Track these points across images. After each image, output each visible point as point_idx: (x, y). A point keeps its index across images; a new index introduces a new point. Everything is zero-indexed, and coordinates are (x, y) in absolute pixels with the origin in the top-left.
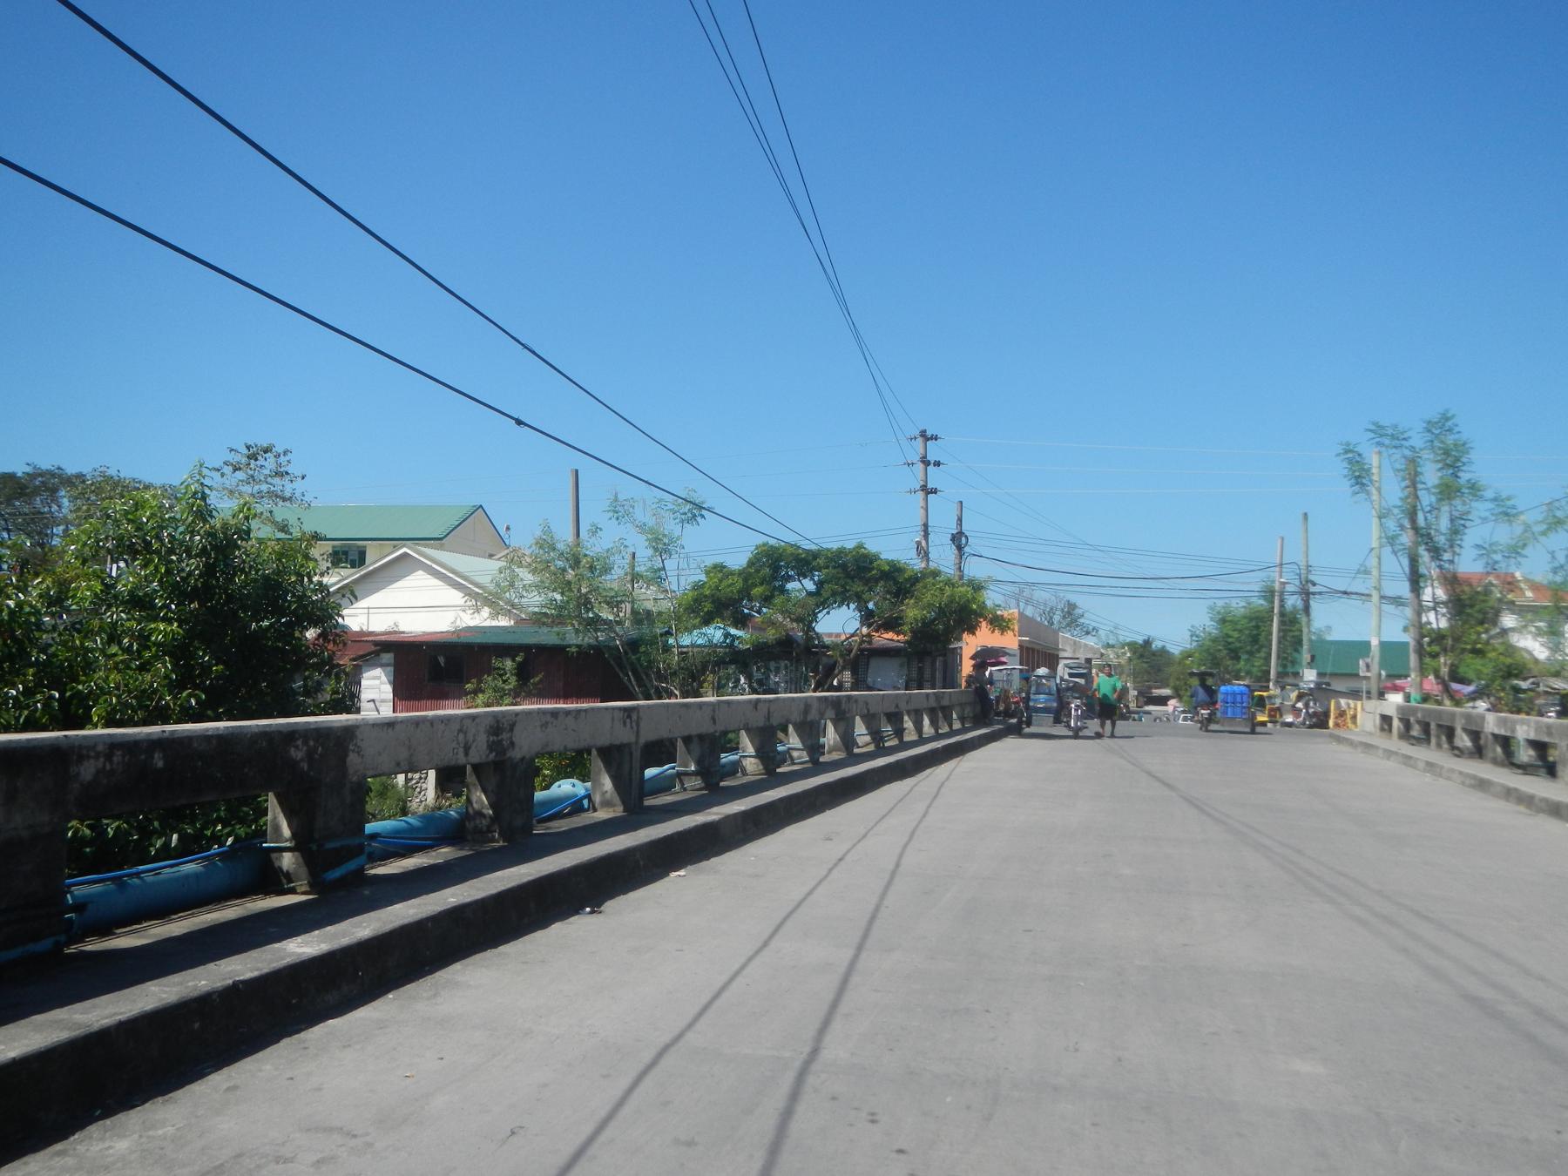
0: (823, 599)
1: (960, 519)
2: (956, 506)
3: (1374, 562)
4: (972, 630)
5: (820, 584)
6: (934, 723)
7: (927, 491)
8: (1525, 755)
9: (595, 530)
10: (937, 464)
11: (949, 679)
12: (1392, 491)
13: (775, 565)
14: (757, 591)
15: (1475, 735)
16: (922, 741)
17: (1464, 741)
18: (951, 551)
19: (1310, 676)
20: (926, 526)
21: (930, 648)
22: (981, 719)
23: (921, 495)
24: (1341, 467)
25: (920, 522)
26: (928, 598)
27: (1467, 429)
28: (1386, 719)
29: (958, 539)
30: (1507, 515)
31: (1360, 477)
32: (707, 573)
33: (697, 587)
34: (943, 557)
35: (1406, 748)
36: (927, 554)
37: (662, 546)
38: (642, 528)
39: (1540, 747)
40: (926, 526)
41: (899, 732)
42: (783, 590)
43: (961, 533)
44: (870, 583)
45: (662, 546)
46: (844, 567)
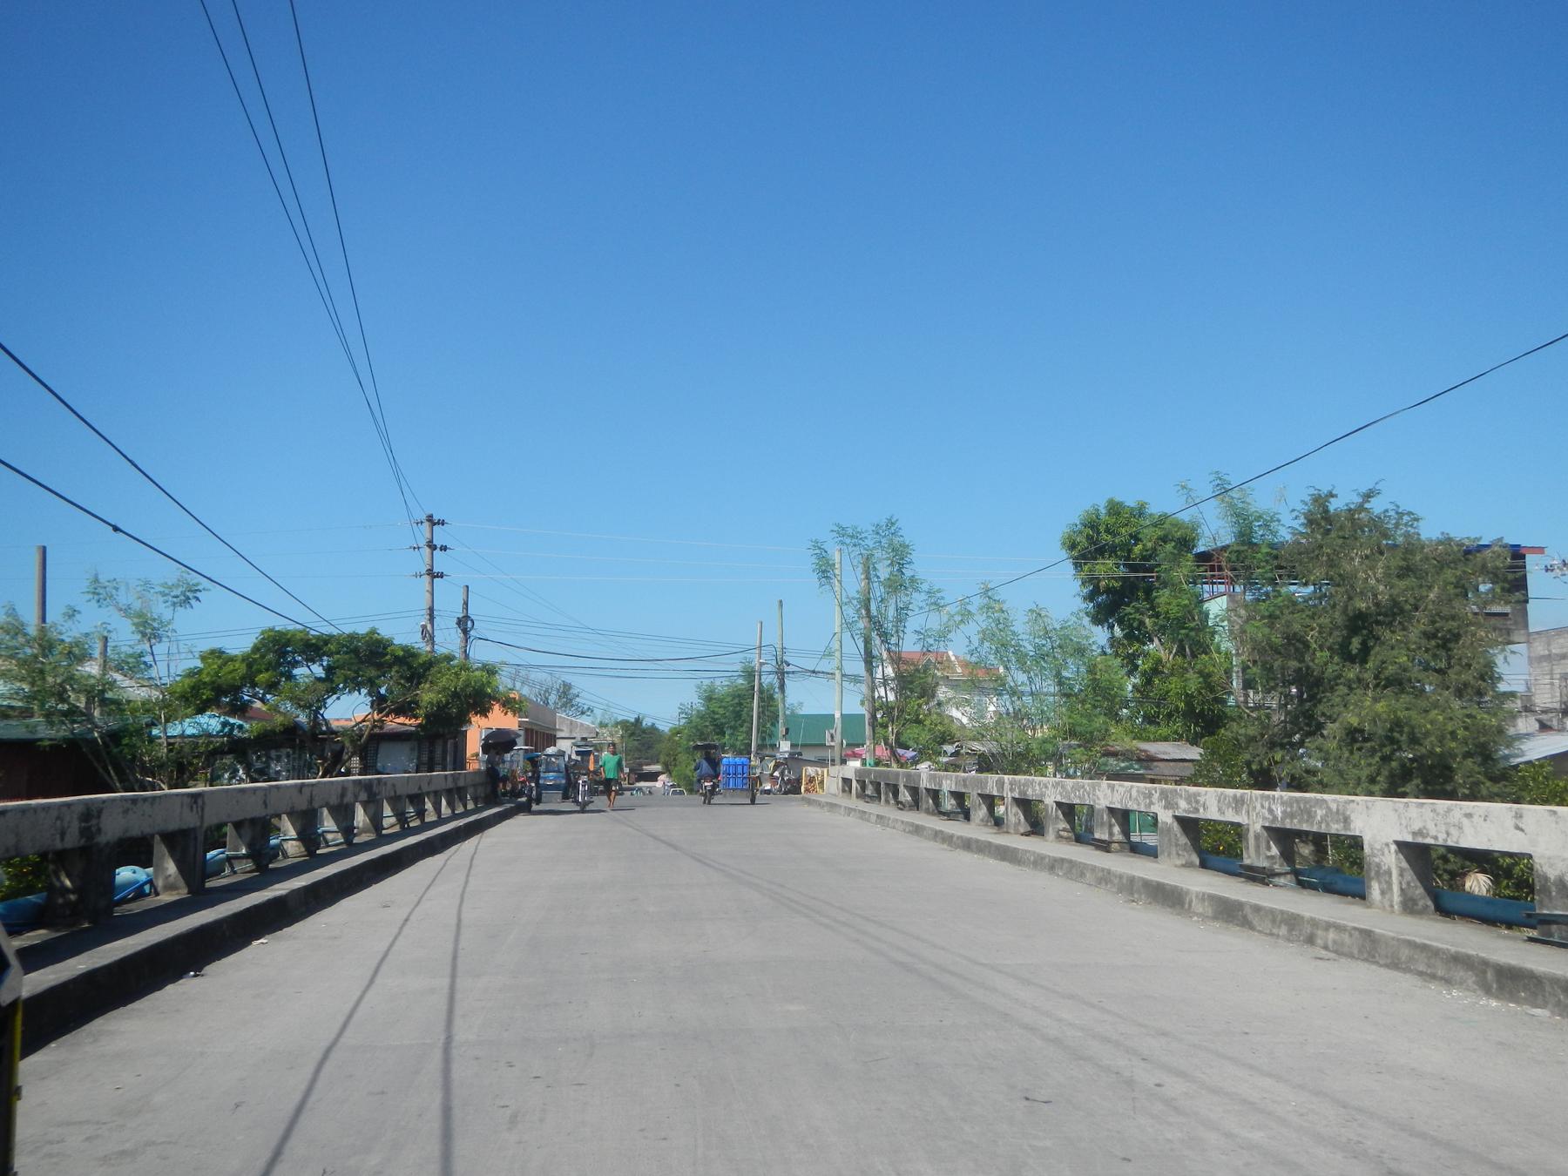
0: (330, 685)
1: (466, 603)
3: (837, 646)
4: (484, 712)
5: (329, 670)
6: (451, 804)
7: (433, 575)
8: (949, 804)
9: (72, 613)
10: (444, 548)
11: (459, 761)
12: (851, 581)
13: (280, 651)
14: (262, 677)
15: (914, 791)
16: (441, 821)
17: (905, 796)
19: (785, 746)
20: (431, 609)
21: (439, 735)
22: (491, 799)
23: (427, 579)
24: (809, 561)
25: (426, 605)
26: (443, 682)
28: (847, 782)
29: (464, 623)
30: (938, 606)
31: (825, 571)
32: (203, 658)
33: (192, 673)
34: (448, 641)
35: (862, 805)
36: (432, 638)
37: (149, 630)
38: (126, 611)
39: (959, 797)
40: (431, 609)
41: (421, 813)
42: (290, 677)
43: (467, 617)
44: (383, 668)
45: (149, 630)
46: (356, 651)
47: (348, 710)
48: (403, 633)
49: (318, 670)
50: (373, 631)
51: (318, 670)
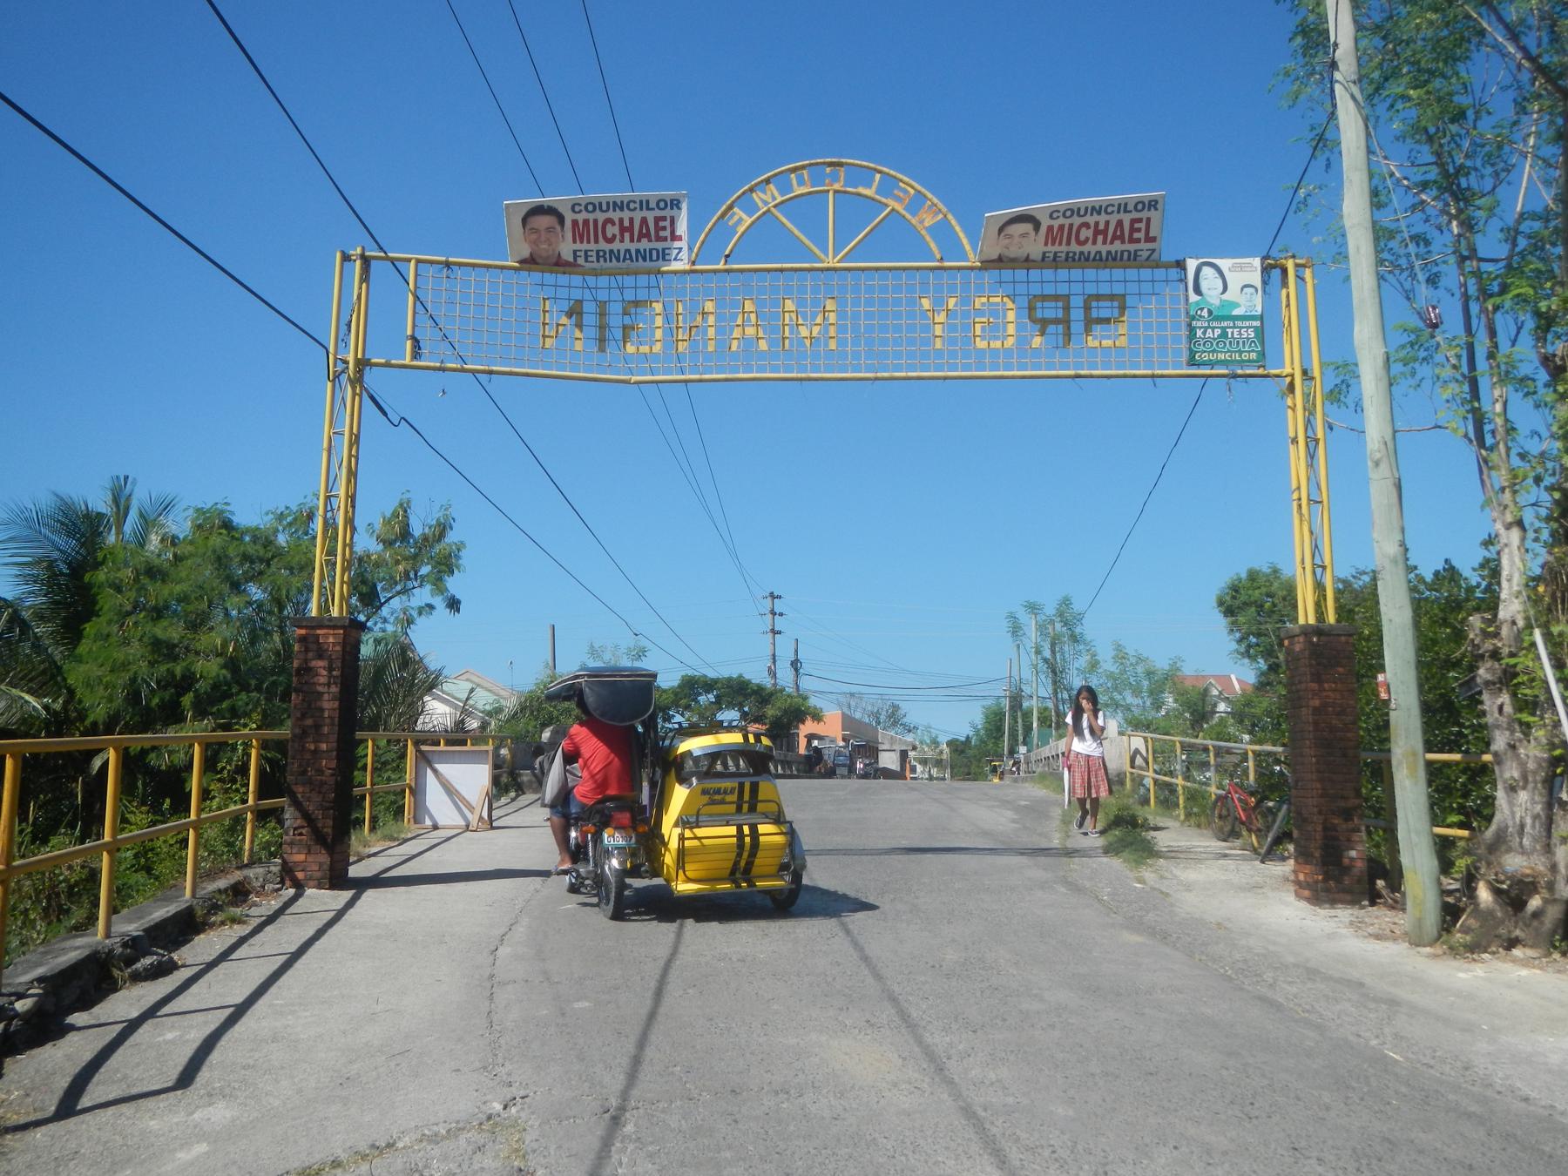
0: (719, 704)
7: (774, 632)
14: (683, 702)
18: (791, 673)
29: (796, 664)
31: (1016, 630)
34: (785, 678)
44: (746, 696)
48: (757, 675)
49: (711, 697)
50: (741, 676)
51: (711, 697)
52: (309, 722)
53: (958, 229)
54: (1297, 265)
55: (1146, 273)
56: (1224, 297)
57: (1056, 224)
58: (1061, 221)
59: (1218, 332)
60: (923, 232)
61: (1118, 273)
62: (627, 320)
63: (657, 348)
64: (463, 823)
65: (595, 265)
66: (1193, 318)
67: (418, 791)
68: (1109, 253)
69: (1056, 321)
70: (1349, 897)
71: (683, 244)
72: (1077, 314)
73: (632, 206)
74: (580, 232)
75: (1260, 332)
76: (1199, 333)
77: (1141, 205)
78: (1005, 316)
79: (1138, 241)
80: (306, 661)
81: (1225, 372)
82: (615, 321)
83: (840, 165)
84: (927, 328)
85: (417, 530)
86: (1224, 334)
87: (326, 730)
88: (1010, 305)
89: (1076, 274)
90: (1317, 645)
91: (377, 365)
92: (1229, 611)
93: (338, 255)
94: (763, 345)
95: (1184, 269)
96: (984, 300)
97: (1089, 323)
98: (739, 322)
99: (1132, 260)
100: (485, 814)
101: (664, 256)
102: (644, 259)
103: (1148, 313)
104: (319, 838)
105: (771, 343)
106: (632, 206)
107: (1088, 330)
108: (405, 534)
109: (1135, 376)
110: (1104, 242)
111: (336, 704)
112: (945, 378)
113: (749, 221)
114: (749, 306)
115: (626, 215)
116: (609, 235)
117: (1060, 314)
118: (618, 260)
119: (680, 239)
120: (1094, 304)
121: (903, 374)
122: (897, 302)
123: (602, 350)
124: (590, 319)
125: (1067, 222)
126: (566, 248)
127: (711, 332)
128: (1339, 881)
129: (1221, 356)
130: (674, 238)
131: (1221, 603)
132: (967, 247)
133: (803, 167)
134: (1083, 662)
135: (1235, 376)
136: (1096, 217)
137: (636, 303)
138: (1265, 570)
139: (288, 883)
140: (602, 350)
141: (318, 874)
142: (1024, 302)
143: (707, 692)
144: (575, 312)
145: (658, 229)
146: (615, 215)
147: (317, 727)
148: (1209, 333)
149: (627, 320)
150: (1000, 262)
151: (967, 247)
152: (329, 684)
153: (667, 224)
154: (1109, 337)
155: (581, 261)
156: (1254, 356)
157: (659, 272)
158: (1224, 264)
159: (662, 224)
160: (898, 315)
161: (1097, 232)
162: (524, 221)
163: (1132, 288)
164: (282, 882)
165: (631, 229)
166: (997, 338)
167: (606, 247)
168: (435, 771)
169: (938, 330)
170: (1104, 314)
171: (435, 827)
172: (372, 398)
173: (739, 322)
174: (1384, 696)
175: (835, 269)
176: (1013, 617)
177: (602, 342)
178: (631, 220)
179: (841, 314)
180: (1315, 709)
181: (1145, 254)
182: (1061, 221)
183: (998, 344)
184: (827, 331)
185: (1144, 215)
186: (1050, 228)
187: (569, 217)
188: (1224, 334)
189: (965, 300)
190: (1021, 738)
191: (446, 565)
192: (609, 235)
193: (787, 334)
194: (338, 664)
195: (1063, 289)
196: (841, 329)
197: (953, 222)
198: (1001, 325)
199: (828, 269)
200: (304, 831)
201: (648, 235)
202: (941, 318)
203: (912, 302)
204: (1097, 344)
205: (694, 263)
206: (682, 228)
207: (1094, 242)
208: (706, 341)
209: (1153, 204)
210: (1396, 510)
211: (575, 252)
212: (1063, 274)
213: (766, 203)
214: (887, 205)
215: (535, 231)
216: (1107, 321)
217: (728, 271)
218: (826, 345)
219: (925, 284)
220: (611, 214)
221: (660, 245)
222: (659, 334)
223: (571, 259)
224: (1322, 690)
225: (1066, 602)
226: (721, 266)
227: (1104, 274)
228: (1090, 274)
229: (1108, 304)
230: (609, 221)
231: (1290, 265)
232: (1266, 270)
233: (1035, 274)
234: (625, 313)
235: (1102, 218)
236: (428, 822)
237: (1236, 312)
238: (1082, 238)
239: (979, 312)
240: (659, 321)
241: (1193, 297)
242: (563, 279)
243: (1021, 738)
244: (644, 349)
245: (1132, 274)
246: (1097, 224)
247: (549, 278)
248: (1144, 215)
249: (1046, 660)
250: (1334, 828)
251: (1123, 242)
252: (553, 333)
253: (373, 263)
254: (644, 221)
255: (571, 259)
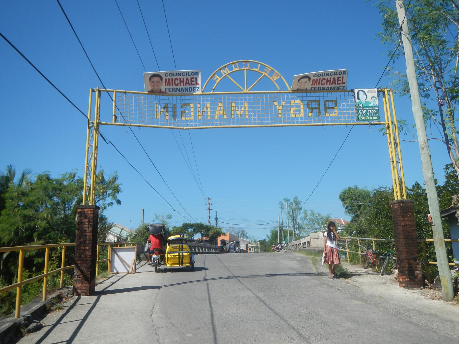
0: (195, 232)
2: (215, 212)
4: (220, 236)
7: (209, 209)
11: (216, 244)
13: (186, 226)
14: (184, 231)
21: (213, 239)
25: (208, 216)
26: (213, 231)
27: (299, 200)
29: (216, 219)
31: (282, 207)
32: (173, 228)
34: (213, 223)
38: (160, 220)
42: (188, 231)
43: (216, 218)
44: (203, 229)
46: (198, 226)
47: (197, 236)
48: (205, 222)
49: (192, 229)
51: (192, 229)
52: (82, 240)
53: (284, 81)
54: (388, 91)
55: (342, 94)
56: (367, 100)
57: (315, 78)
58: (317, 78)
59: (365, 111)
60: (274, 82)
61: (334, 94)
62: (183, 110)
63: (192, 118)
64: (126, 271)
65: (172, 93)
66: (358, 107)
67: (112, 261)
68: (331, 87)
69: (316, 108)
70: (417, 286)
71: (200, 86)
72: (322, 106)
73: (184, 74)
74: (168, 82)
75: (378, 111)
76: (360, 111)
77: (341, 73)
78: (300, 107)
79: (340, 84)
80: (81, 220)
81: (368, 123)
82: (178, 110)
83: (248, 62)
84: (276, 111)
85: (106, 179)
86: (367, 112)
87: (88, 242)
88: (301, 103)
89: (321, 94)
90: (402, 206)
91: (103, 124)
92: (343, 200)
93: (91, 90)
94: (225, 117)
95: (354, 92)
96: (293, 102)
97: (326, 109)
98: (218, 110)
99: (338, 90)
100: (134, 269)
101: (194, 90)
102: (187, 91)
103: (343, 106)
104: (86, 278)
105: (228, 116)
106: (184, 74)
107: (326, 111)
108: (103, 181)
109: (341, 125)
110: (330, 84)
111: (91, 234)
112: (283, 126)
113: (220, 79)
114: (221, 105)
115: (182, 77)
116: (176, 83)
117: (317, 106)
118: (179, 91)
119: (198, 84)
120: (327, 103)
121: (269, 125)
122: (267, 103)
123: (174, 119)
124: (170, 109)
125: (318, 78)
126: (163, 87)
127: (209, 113)
128: (414, 281)
129: (367, 118)
130: (197, 84)
131: (340, 197)
132: (288, 86)
133: (236, 63)
134: (302, 216)
135: (371, 124)
136: (327, 77)
137: (185, 104)
138: (354, 187)
139: (75, 294)
140: (174, 119)
141: (86, 291)
142: (306, 102)
143: (191, 228)
144: (166, 107)
145: (192, 81)
146: (178, 77)
147: (85, 241)
148: (363, 111)
149: (183, 110)
150: (298, 91)
151: (288, 86)
152: (89, 227)
153: (194, 80)
154: (332, 113)
155: (167, 91)
156: (376, 118)
157: (192, 95)
158: (366, 90)
159: (193, 80)
160: (267, 107)
161: (327, 81)
162: (150, 79)
163: (338, 98)
164: (73, 294)
165: (183, 81)
166: (298, 114)
167: (175, 87)
168: (117, 255)
169: (280, 112)
170: (330, 106)
171: (118, 273)
172: (101, 135)
173: (218, 110)
174: (430, 221)
175: (247, 93)
176: (281, 203)
177: (174, 116)
178: (183, 79)
179: (250, 107)
180: (403, 226)
181: (342, 88)
182: (317, 78)
183: (298, 115)
184: (245, 112)
185: (342, 76)
186: (314, 80)
187: (164, 78)
188: (367, 112)
189: (288, 102)
190: (283, 239)
191: (116, 190)
192: (176, 83)
193: (233, 113)
194: (92, 220)
195: (317, 99)
196: (250, 112)
197: (283, 79)
198: (299, 110)
199: (245, 93)
200: (80, 276)
201: (188, 83)
202: (280, 108)
203: (271, 103)
204: (328, 115)
205: (203, 92)
206: (199, 81)
207: (327, 84)
208: (207, 116)
209: (344, 73)
210: (430, 163)
211: (166, 89)
212: (317, 94)
213: (225, 73)
214: (262, 74)
215: (154, 82)
216: (331, 108)
217: (214, 94)
218: (245, 116)
219: (275, 98)
220: (177, 77)
221: (192, 86)
222: (192, 114)
223: (164, 91)
224: (404, 220)
225: (296, 198)
226: (211, 93)
227: (330, 94)
228: (325, 94)
229: (331, 103)
230: (177, 79)
231: (386, 90)
232: (378, 92)
233: (309, 94)
234: (181, 108)
235: (329, 77)
236: (115, 271)
237: (370, 105)
238: (323, 83)
239: (292, 106)
240: (192, 110)
241: (357, 101)
242: (162, 97)
243: (283, 239)
244: (188, 118)
245: (338, 94)
246: (327, 78)
247: (158, 97)
248: (342, 76)
249: (291, 216)
250: (411, 264)
251: (335, 84)
252: (159, 114)
253: (102, 92)
254: (187, 79)
255: (164, 91)
